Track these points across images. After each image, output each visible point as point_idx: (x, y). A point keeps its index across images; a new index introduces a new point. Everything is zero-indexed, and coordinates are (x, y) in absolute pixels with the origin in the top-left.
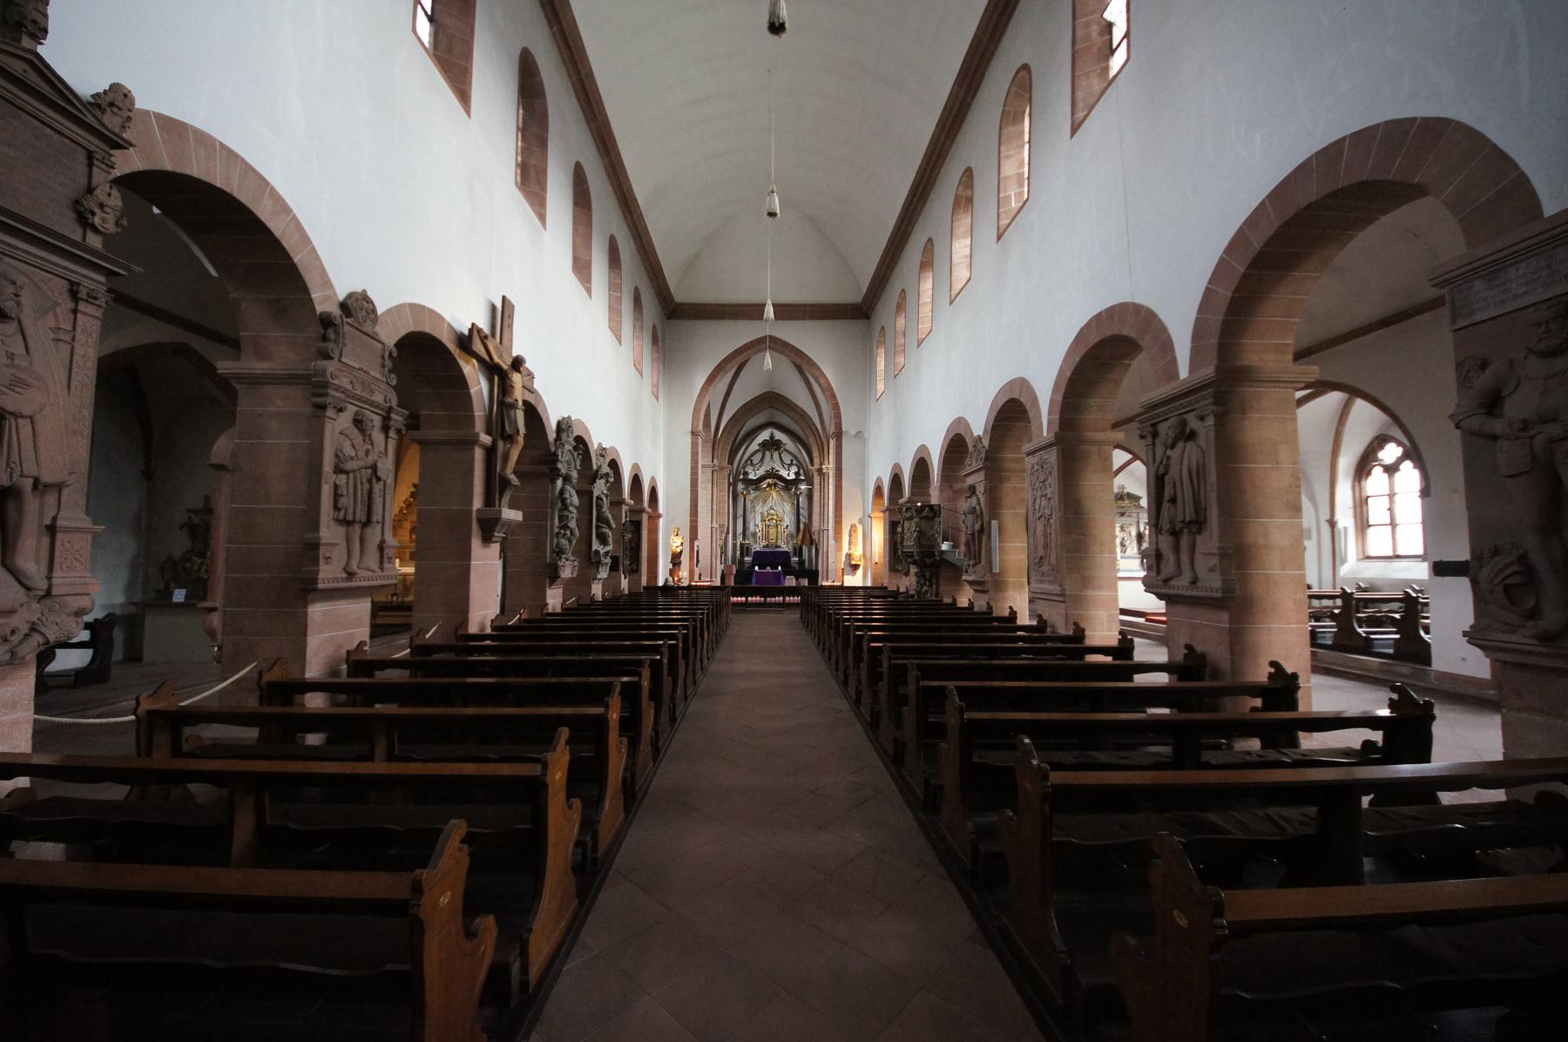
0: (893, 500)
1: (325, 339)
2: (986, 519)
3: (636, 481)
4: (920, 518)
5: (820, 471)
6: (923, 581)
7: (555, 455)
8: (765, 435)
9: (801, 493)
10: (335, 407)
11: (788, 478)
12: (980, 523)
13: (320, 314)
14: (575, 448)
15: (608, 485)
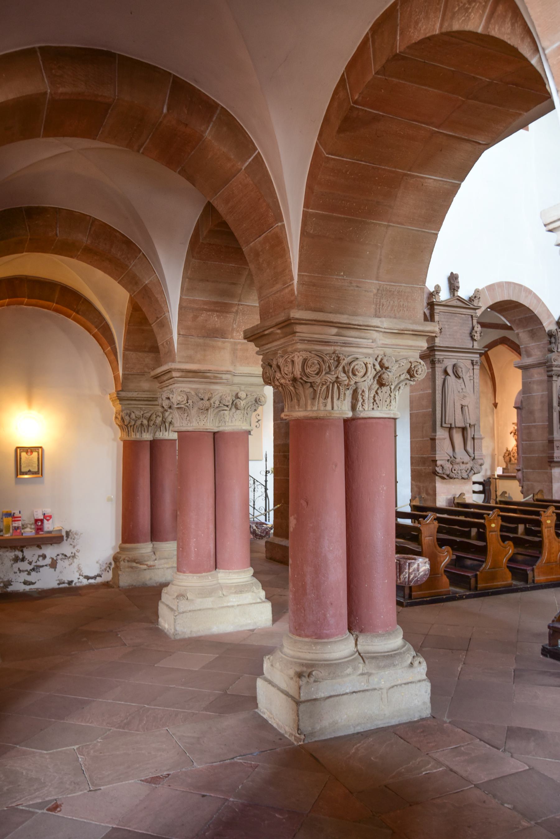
1: (550, 343)
10: (556, 375)
13: (548, 331)
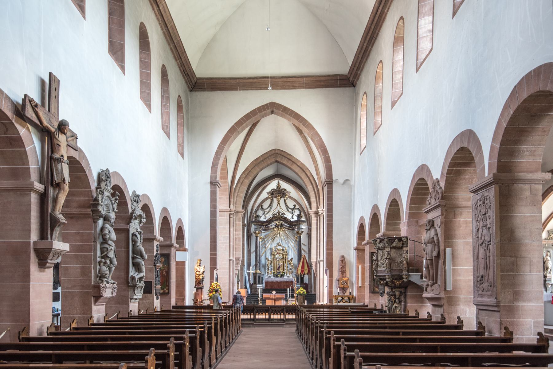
0: (372, 234)
2: (442, 248)
3: (166, 221)
4: (391, 248)
5: (316, 213)
6: (393, 299)
7: (96, 200)
8: (273, 185)
9: (302, 232)
11: (292, 220)
12: (437, 249)
14: (113, 195)
15: (142, 224)
